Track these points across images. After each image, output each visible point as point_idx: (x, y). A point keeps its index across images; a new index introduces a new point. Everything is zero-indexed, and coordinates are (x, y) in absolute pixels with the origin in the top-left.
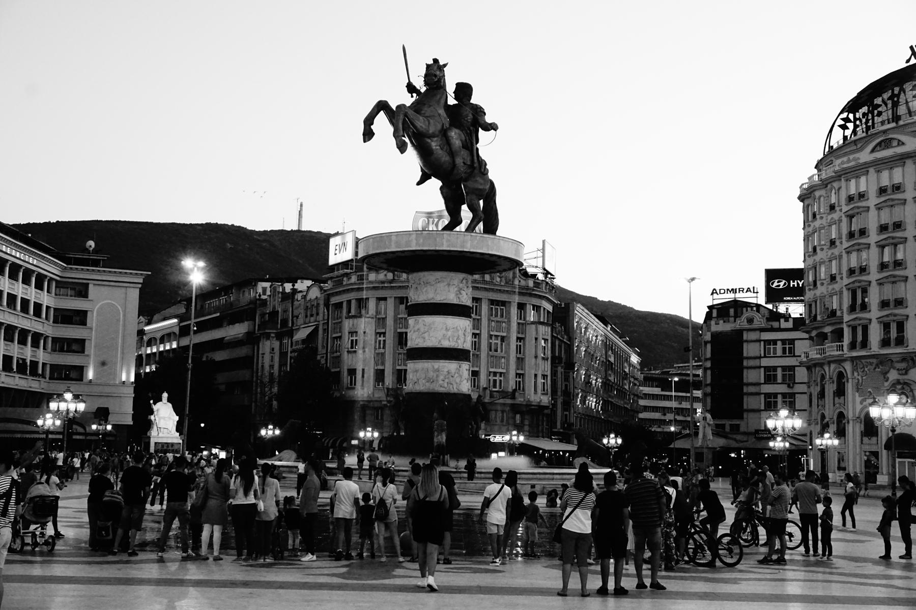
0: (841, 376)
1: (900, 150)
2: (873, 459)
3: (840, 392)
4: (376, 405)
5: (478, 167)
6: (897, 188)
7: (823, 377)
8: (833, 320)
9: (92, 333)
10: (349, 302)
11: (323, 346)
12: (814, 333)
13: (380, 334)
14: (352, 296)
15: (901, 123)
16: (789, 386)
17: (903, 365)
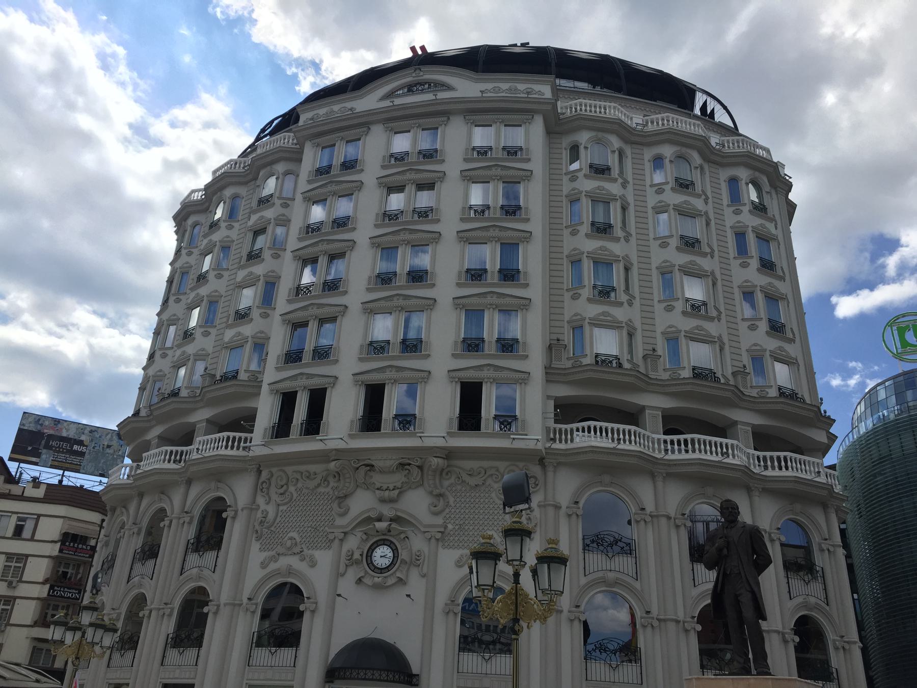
7: (161, 514)
16: (10, 585)
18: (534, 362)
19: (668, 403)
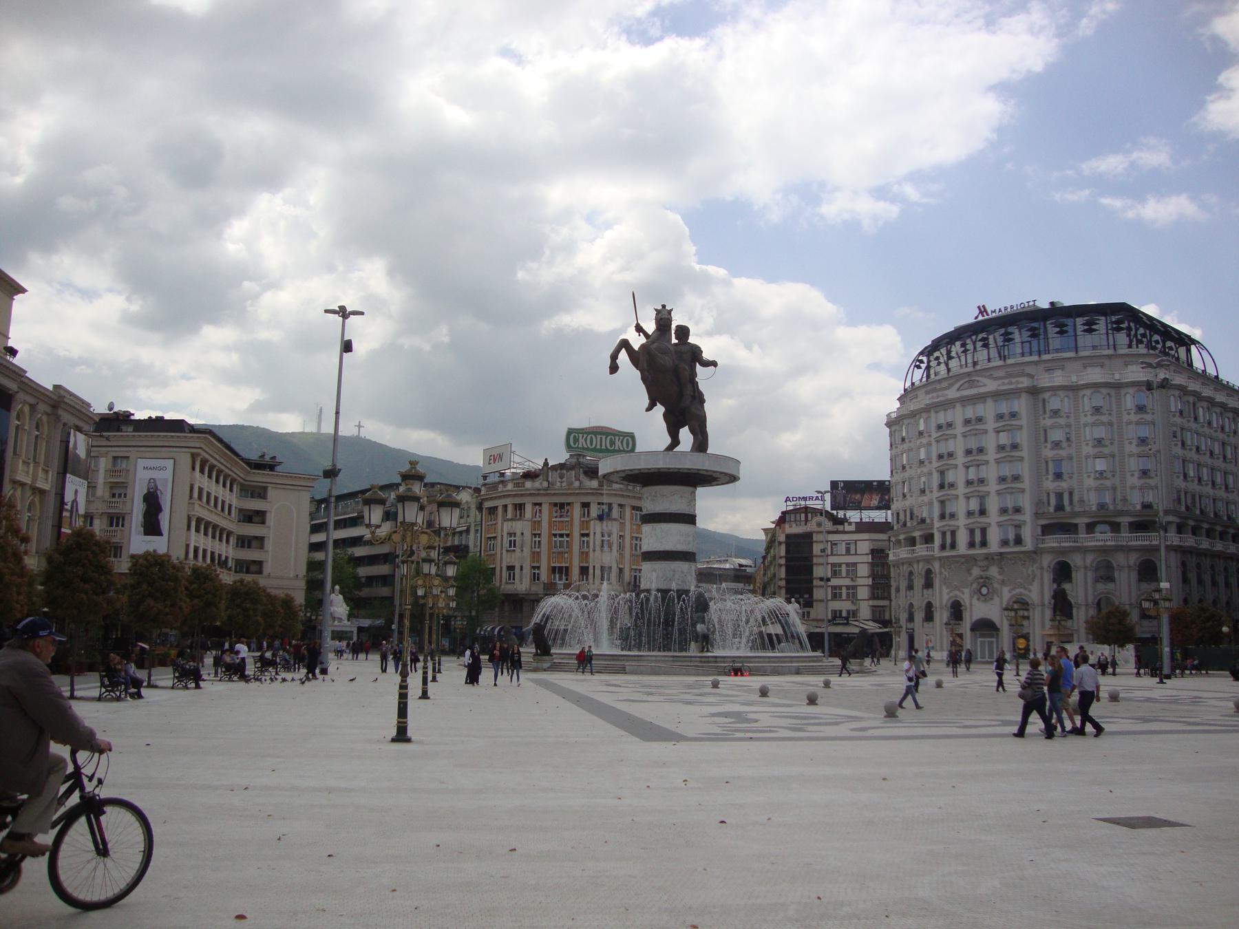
0: (911, 573)
2: (958, 640)
3: (929, 584)
4: (533, 598)
5: (699, 399)
6: (980, 420)
7: (911, 573)
8: (923, 526)
9: (269, 530)
10: (505, 507)
11: (475, 546)
12: (902, 537)
13: (535, 535)
14: (508, 501)
15: (978, 367)
17: (985, 563)
18: (1027, 516)
19: (1087, 520)
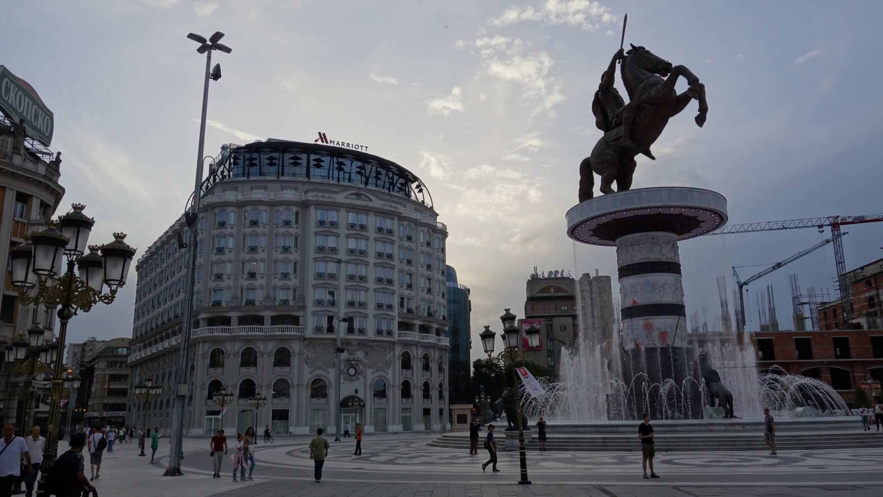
1: (370, 204)
19: (421, 323)
